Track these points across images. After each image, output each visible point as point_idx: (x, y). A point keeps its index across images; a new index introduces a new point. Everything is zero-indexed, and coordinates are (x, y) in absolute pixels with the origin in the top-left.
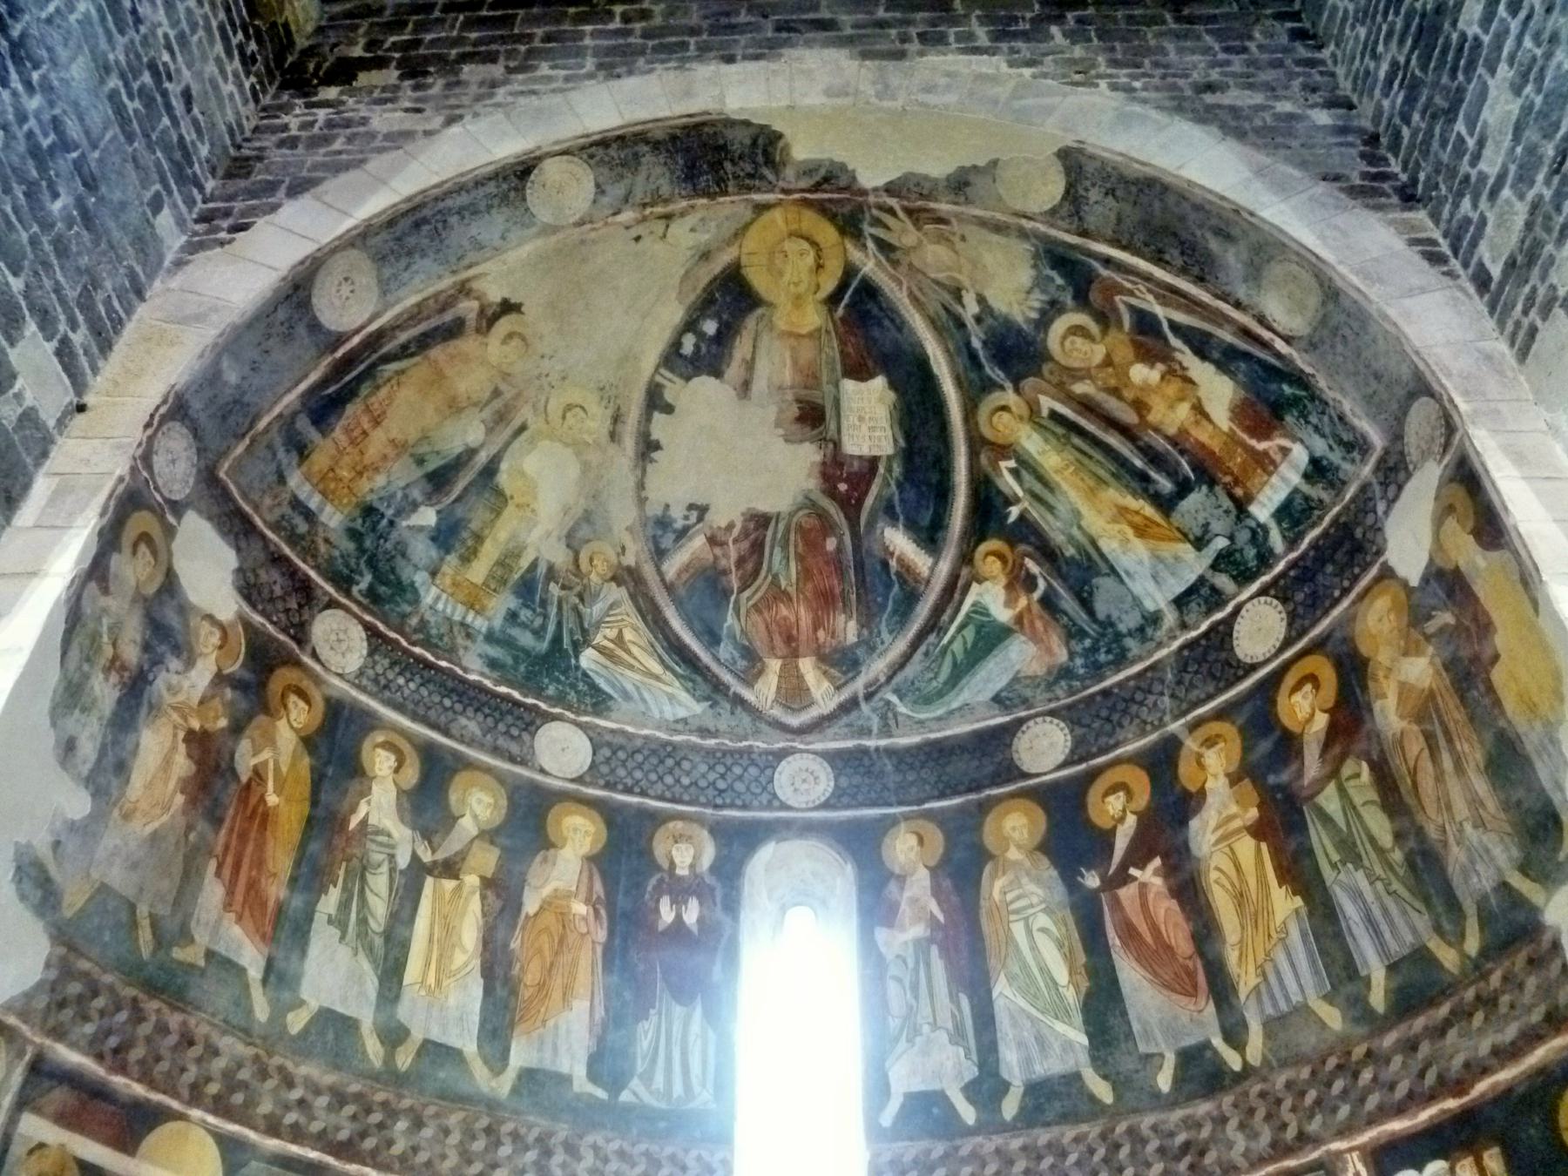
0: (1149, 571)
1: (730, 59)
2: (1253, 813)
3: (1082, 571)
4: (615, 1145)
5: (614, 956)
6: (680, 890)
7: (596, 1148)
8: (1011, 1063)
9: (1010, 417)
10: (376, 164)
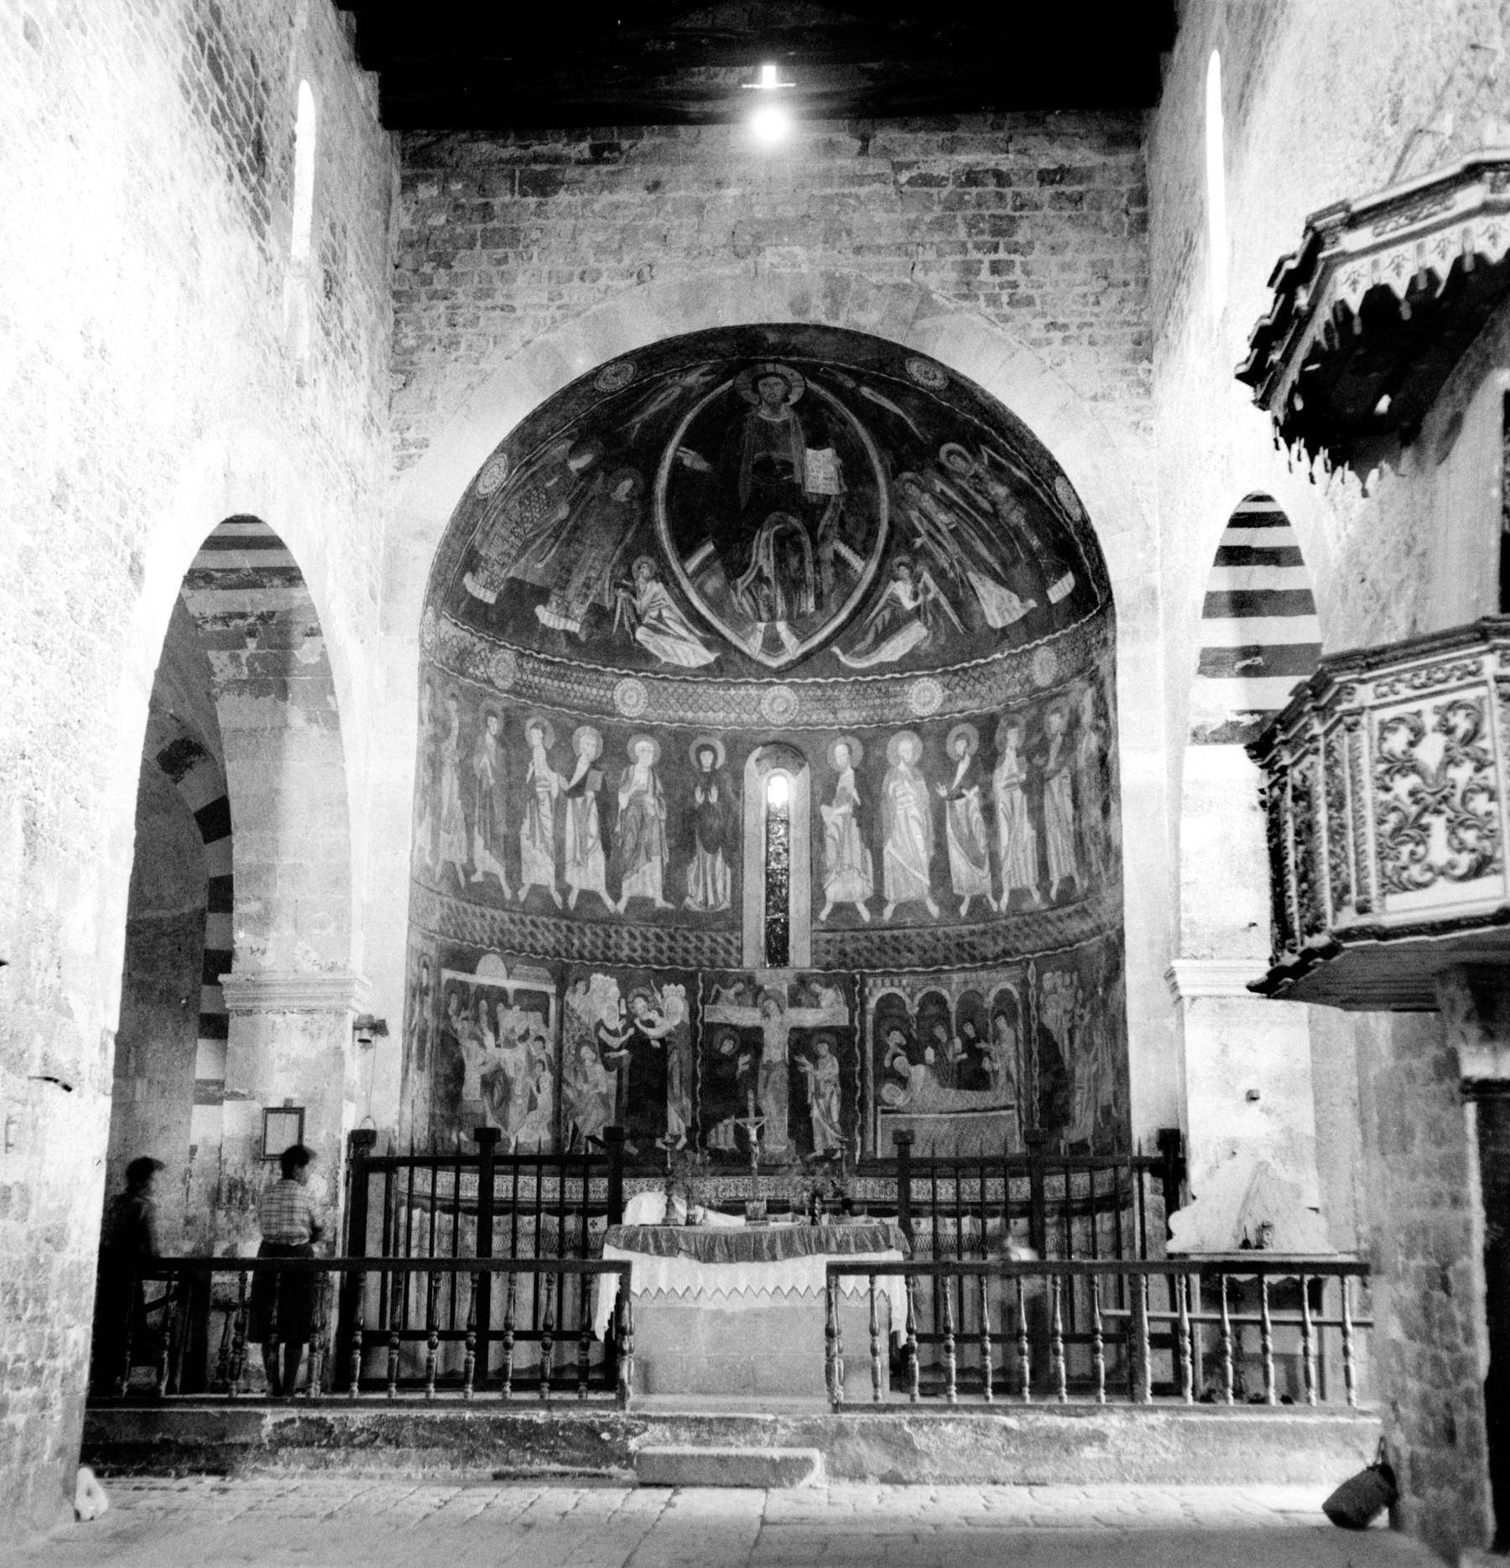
2: (1023, 777)
8: (890, 893)
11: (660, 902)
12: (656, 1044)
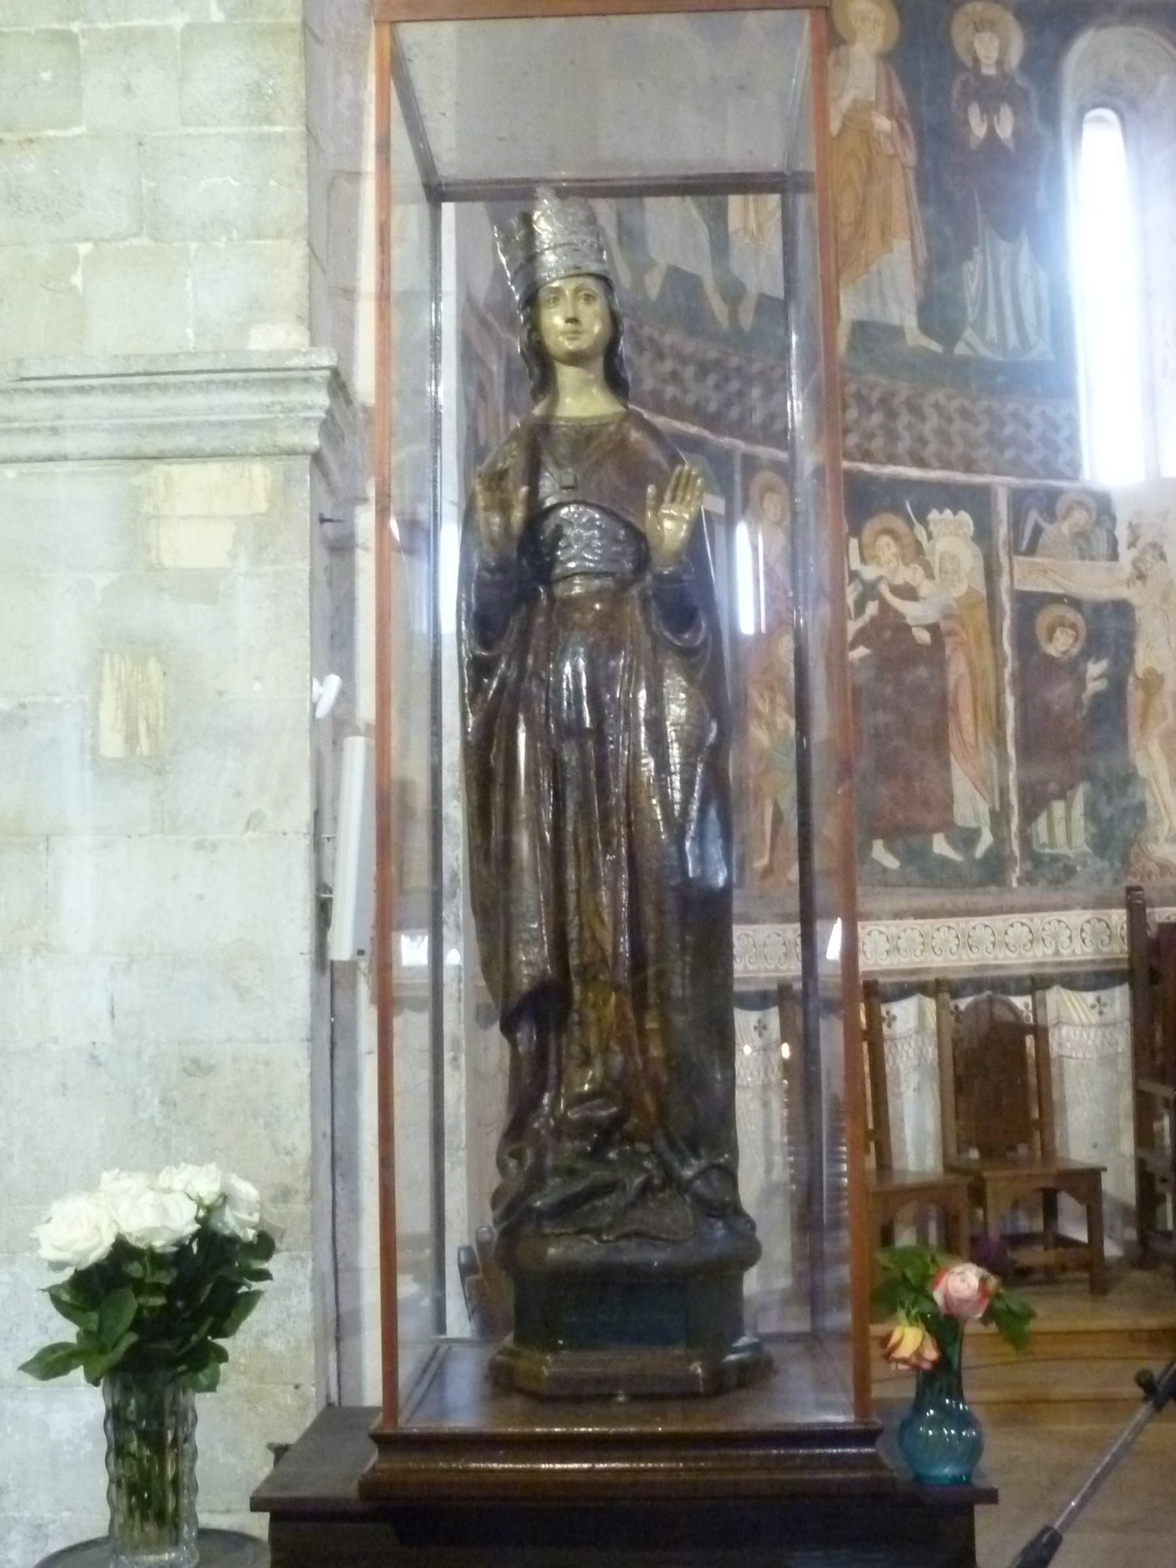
4: (955, 404)
6: (991, 94)
7: (937, 406)
11: (914, 337)
12: (924, 637)
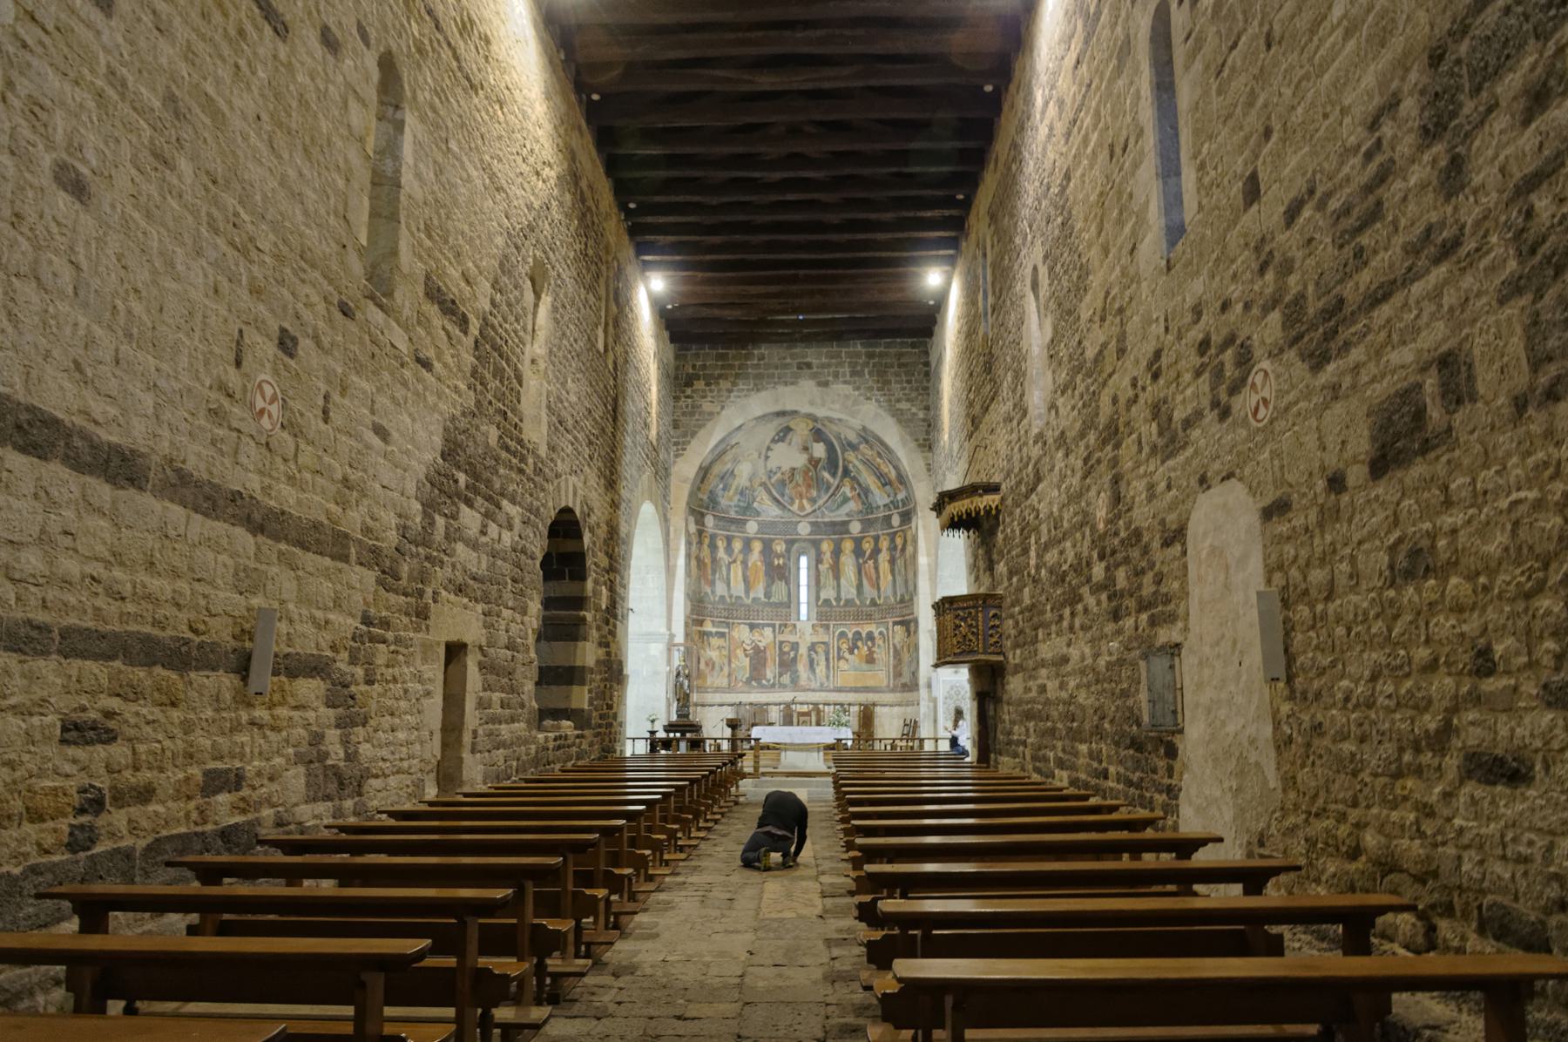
0: (880, 497)
1: (786, 384)
3: (866, 491)
5: (766, 574)
6: (779, 556)
8: (843, 595)
9: (851, 456)
10: (709, 425)
